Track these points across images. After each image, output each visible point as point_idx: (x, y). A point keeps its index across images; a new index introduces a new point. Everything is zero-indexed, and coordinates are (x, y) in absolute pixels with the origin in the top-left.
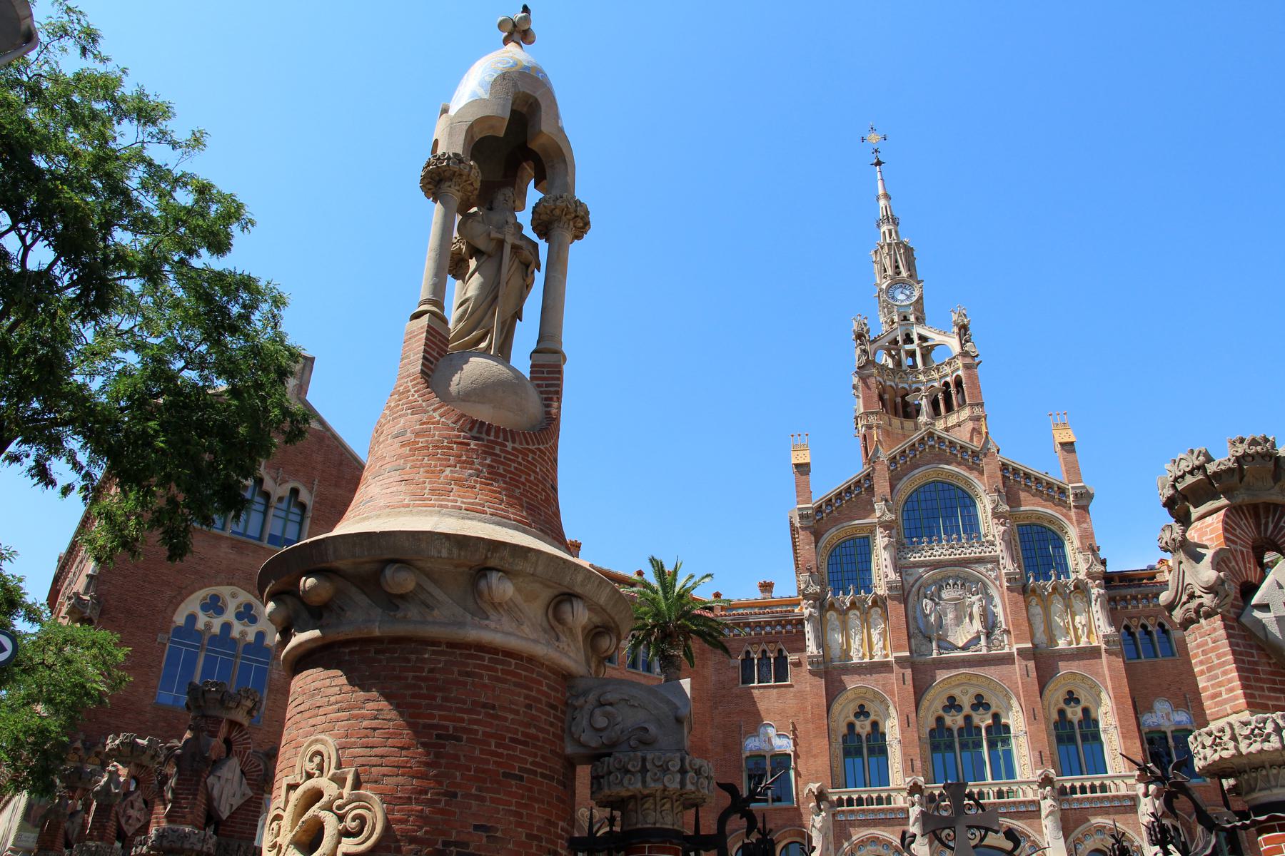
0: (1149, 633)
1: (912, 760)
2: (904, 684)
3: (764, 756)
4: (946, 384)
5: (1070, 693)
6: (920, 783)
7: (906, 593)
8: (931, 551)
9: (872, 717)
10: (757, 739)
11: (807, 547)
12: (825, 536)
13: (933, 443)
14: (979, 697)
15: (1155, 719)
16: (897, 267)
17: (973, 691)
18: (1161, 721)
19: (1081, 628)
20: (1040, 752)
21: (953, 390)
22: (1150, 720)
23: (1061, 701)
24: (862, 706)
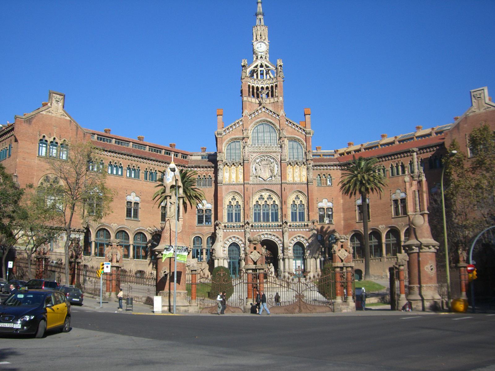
4: (272, 87)
5: (297, 196)
13: (264, 110)
14: (270, 195)
16: (261, 35)
18: (324, 205)
21: (274, 90)
22: (320, 205)
23: (294, 198)
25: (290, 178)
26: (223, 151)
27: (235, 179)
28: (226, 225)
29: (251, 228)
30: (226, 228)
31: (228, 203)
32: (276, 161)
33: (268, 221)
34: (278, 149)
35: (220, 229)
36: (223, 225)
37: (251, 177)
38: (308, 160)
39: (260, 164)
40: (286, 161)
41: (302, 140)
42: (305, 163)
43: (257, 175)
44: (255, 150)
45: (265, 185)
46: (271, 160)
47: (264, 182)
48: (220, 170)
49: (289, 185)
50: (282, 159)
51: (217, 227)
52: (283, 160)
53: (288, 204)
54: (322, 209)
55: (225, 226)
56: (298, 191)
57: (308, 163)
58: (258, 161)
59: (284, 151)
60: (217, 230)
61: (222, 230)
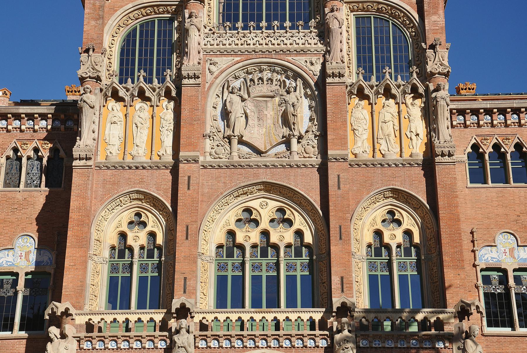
0: (502, 156)
1: (185, 279)
2: (189, 189)
3: (17, 275)
6: (188, 306)
7: (207, 85)
8: (244, 39)
9: (149, 228)
10: (11, 252)
11: (93, 23)
12: (119, 13)
14: (281, 210)
15: (494, 255)
17: (273, 205)
19: (414, 137)
20: (342, 278)
23: (379, 220)
24: (138, 215)
25: (359, 144)
26: (106, 44)
27: (144, 146)
28: (95, 319)
29: (198, 333)
30: (95, 333)
31: (113, 239)
32: (306, 84)
33: (273, 303)
34: (312, 42)
35: (63, 336)
36: (81, 320)
37: (208, 140)
38: (432, 74)
39: (246, 96)
40: (342, 80)
41: (408, 8)
42: (421, 90)
43: (229, 132)
44: (227, 46)
45: (261, 171)
46: (288, 82)
47: (255, 159)
48: (86, 109)
49: (356, 169)
50: (329, 71)
51: (54, 331)
52: (334, 75)
53: (353, 241)
54: (494, 275)
55: (90, 327)
56: (395, 191)
57: (432, 87)
58: (237, 84)
59: (336, 45)
60: (51, 341)
61: (76, 343)
